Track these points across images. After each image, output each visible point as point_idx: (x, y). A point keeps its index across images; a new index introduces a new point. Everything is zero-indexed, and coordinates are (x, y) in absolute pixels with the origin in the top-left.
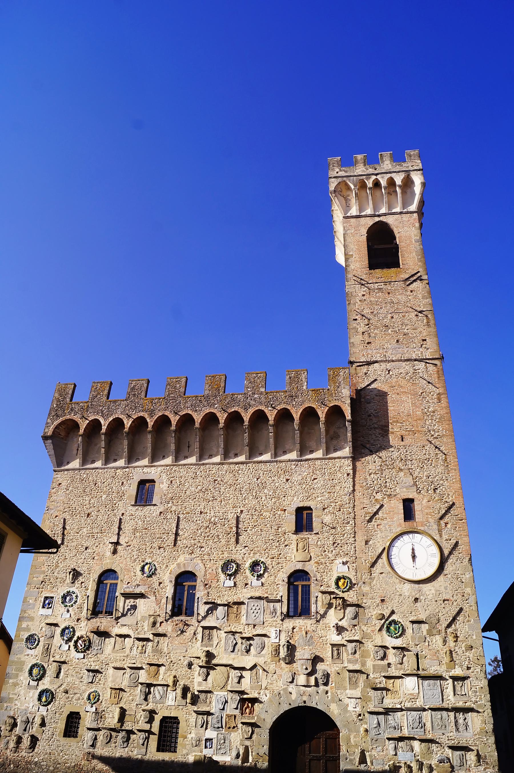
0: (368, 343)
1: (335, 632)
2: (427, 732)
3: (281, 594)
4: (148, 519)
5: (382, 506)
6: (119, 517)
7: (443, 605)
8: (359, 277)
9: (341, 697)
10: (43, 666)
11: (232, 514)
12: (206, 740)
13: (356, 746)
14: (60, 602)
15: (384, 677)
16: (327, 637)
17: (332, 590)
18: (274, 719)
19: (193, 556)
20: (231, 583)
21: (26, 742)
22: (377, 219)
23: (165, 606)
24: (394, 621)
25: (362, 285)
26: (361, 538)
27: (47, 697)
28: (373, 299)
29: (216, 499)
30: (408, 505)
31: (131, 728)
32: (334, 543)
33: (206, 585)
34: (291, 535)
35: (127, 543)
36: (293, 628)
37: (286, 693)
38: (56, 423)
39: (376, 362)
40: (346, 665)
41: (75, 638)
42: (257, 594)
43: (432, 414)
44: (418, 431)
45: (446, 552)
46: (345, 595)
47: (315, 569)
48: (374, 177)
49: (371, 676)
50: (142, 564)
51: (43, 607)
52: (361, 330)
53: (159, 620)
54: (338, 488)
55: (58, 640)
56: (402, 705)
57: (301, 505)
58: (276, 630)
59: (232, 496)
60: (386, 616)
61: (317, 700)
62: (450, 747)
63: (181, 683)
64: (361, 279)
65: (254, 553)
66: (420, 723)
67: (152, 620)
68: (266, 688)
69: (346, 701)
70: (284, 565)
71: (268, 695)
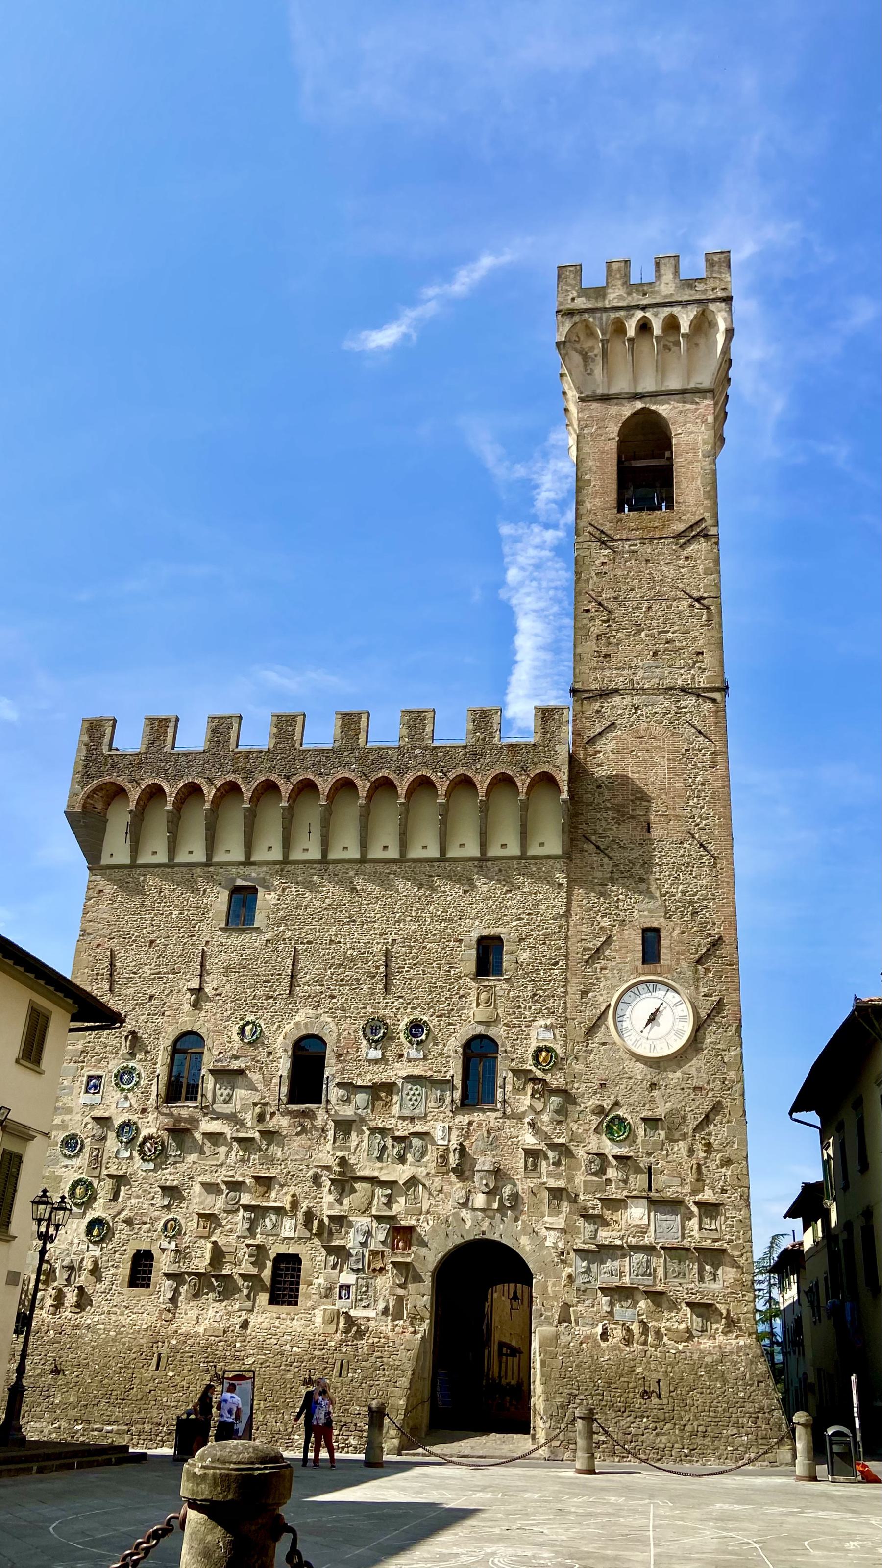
0: (606, 656)
1: (530, 1130)
2: (658, 1281)
3: (451, 1072)
4: (248, 951)
5: (609, 940)
6: (200, 948)
7: (692, 1096)
8: (599, 527)
9: (538, 1227)
10: (91, 1184)
11: (380, 946)
12: (341, 1287)
13: (556, 1297)
14: (113, 1083)
15: (599, 1199)
16: (520, 1138)
17: (529, 1068)
18: (440, 1256)
19: (320, 1011)
20: (375, 1054)
21: (71, 1298)
22: (639, 405)
23: (277, 1088)
24: (617, 1117)
25: (603, 543)
26: (574, 989)
27: (99, 1230)
28: (619, 573)
29: (354, 921)
30: (651, 939)
31: (229, 1273)
32: (535, 995)
33: (341, 1055)
34: (469, 980)
35: (216, 990)
36: (470, 1123)
37: (457, 1220)
38: (88, 788)
39: (616, 691)
40: (545, 1180)
41: (140, 1139)
42: (417, 1072)
43: (700, 787)
44: (677, 817)
45: (703, 1014)
46: (548, 1077)
47: (504, 1035)
48: (639, 314)
49: (582, 1197)
50: (241, 1023)
51: (87, 1092)
52: (595, 631)
53: (269, 1110)
54: (543, 907)
55: (112, 1143)
57: (486, 932)
58: (442, 1127)
59: (378, 916)
60: (607, 1108)
61: (503, 1232)
62: (688, 1304)
63: (304, 1206)
64: (602, 532)
65: (412, 1008)
66: (648, 1267)
67: (258, 1110)
68: (428, 1212)
69: (544, 1232)
70: (457, 1027)
71: (431, 1222)
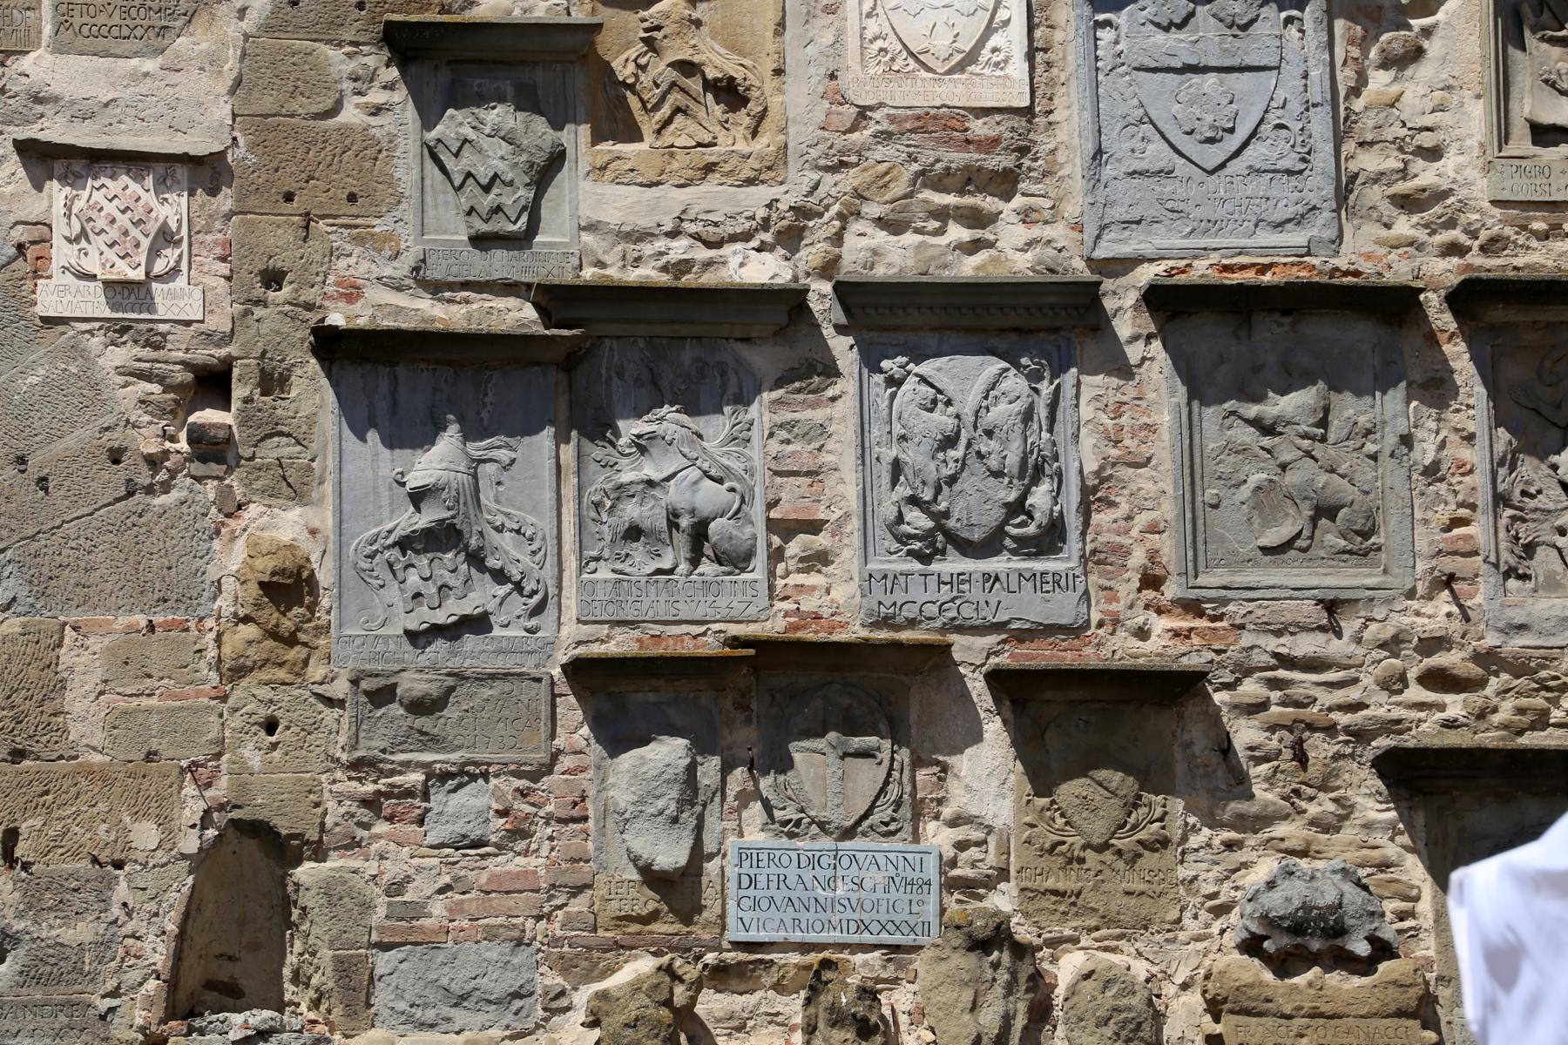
13: (143, 776)
56: (812, 253)
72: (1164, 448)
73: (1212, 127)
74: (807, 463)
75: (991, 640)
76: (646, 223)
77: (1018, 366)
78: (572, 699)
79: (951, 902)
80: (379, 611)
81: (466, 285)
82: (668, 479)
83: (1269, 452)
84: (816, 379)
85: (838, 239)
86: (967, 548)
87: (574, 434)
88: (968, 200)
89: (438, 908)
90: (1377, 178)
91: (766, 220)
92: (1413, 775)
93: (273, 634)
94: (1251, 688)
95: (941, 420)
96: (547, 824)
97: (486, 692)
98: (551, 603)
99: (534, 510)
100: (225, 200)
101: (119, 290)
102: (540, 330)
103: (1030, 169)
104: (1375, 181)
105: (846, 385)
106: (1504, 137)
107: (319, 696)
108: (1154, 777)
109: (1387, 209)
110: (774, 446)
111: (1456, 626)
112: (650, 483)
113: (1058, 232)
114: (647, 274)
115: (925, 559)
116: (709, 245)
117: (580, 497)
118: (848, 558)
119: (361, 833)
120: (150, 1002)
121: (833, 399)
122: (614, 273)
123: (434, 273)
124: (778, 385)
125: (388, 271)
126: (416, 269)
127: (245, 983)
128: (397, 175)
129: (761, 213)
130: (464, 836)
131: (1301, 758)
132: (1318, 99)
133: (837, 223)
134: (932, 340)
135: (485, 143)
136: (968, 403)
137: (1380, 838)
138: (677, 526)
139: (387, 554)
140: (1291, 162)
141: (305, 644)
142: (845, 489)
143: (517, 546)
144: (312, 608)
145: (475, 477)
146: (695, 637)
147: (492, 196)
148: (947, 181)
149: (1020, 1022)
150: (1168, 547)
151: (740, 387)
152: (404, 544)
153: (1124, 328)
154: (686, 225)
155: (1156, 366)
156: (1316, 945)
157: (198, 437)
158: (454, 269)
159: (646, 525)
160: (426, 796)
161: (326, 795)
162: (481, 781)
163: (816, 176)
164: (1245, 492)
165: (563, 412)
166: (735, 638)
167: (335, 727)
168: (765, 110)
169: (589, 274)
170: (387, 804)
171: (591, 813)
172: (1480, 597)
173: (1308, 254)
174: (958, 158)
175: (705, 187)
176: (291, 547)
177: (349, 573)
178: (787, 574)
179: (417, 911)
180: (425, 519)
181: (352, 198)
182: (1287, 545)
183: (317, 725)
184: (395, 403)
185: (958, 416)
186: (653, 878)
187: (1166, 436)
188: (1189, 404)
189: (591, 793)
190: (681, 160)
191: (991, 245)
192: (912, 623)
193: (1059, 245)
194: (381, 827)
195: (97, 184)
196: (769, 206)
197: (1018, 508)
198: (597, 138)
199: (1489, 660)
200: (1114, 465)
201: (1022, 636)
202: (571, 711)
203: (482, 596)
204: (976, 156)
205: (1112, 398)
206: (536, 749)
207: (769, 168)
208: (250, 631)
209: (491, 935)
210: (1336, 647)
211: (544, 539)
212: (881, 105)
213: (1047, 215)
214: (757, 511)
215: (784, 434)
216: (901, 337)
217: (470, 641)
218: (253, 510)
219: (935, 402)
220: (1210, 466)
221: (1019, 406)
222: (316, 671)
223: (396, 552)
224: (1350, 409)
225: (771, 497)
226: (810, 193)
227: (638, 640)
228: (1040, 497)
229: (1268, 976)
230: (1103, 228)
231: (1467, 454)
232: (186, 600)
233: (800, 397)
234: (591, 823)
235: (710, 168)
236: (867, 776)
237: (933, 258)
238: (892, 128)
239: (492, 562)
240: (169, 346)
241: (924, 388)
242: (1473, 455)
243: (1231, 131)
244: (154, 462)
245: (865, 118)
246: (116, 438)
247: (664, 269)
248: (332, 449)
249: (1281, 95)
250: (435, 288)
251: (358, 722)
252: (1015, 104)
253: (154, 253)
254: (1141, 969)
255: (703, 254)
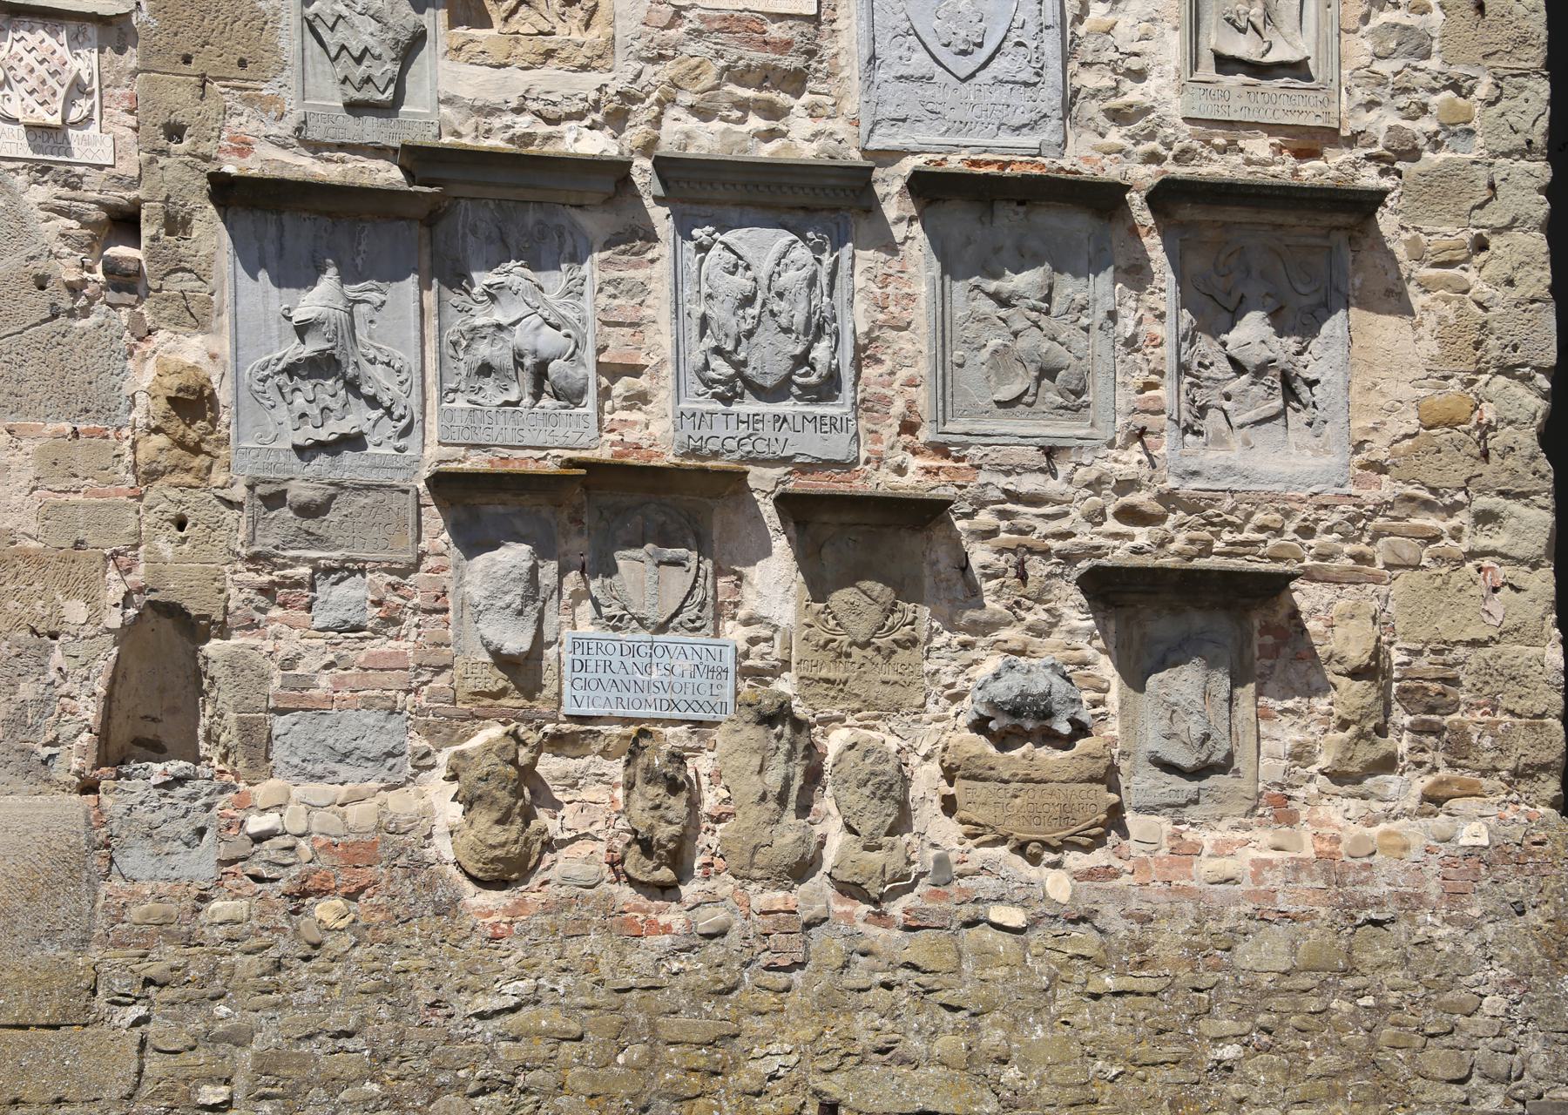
56: (635, 134)
72: (921, 315)
73: (966, 41)
74: (631, 316)
75: (779, 471)
76: (495, 99)
77: (804, 239)
78: (435, 509)
79: (744, 686)
80: (271, 428)
81: (341, 147)
82: (514, 324)
83: (1004, 321)
84: (638, 243)
85: (657, 122)
86: (761, 393)
87: (435, 281)
88: (765, 95)
89: (324, 681)
90: (1095, 94)
91: (597, 102)
92: (1108, 589)
93: (180, 443)
94: (985, 518)
95: (741, 282)
96: (414, 614)
97: (362, 501)
98: (417, 427)
99: (402, 346)
100: (131, 59)
101: (39, 133)
102: (406, 187)
103: (816, 70)
104: (1094, 96)
105: (663, 250)
106: (1195, 65)
107: (221, 499)
108: (908, 589)
109: (1102, 121)
110: (603, 300)
111: (1145, 471)
112: (499, 327)
113: (839, 126)
114: (496, 142)
115: (727, 401)
116: (549, 121)
117: (440, 337)
118: (663, 399)
119: (258, 616)
120: (84, 751)
121: (652, 261)
122: (467, 141)
123: (314, 134)
124: (607, 246)
125: (274, 130)
126: (299, 130)
127: (167, 741)
128: (281, 45)
129: (593, 95)
130: (345, 622)
131: (1023, 576)
132: (1050, 22)
133: (656, 108)
134: (734, 214)
135: (357, 19)
136: (764, 268)
137: (1081, 642)
138: (522, 365)
139: (277, 379)
140: (1028, 75)
141: (208, 454)
142: (661, 338)
143: (388, 377)
144: (214, 422)
145: (351, 314)
146: (537, 461)
147: (363, 67)
148: (748, 77)
149: (797, 783)
150: (923, 398)
151: (575, 247)
152: (291, 370)
153: (891, 210)
154: (529, 103)
155: (916, 246)
156: (1029, 725)
157: (111, 268)
158: (332, 131)
159: (495, 363)
160: (313, 588)
161: (229, 583)
162: (359, 576)
163: (639, 66)
164: (985, 354)
165: (426, 259)
166: (570, 460)
167: (235, 526)
168: (596, 5)
169: (447, 140)
170: (281, 593)
171: (450, 605)
172: (1164, 447)
173: (1039, 155)
174: (757, 57)
175: (545, 71)
176: (193, 368)
177: (245, 394)
178: (614, 410)
179: (306, 683)
180: (310, 348)
181: (242, 63)
182: (1017, 400)
183: (219, 524)
184: (282, 248)
185: (755, 280)
186: (503, 661)
187: (923, 304)
188: (942, 278)
189: (451, 589)
190: (525, 45)
191: (784, 135)
192: (715, 455)
193: (839, 137)
194: (276, 612)
195: (17, 36)
196: (599, 90)
197: (803, 360)
198: (454, 23)
199: (1169, 499)
200: (881, 327)
201: (806, 469)
202: (433, 519)
203: (358, 418)
204: (772, 56)
205: (881, 270)
206: (405, 551)
207: (600, 57)
208: (160, 440)
209: (368, 704)
210: (1052, 486)
211: (410, 371)
212: (694, 6)
213: (830, 110)
214: (589, 355)
215: (610, 290)
216: (709, 210)
217: (348, 457)
218: (161, 336)
219: (736, 266)
220: (957, 330)
221: (806, 273)
222: (218, 477)
223: (284, 378)
224: (1069, 288)
225: (600, 343)
226: (634, 81)
227: (490, 462)
228: (821, 352)
229: (992, 750)
230: (875, 123)
231: (1158, 330)
232: (105, 411)
233: (625, 258)
234: (451, 613)
235: (549, 54)
236: (678, 581)
237: (736, 143)
238: (702, 27)
239: (365, 390)
240: (85, 187)
241: (727, 254)
242: (1164, 331)
243: (980, 45)
244: (74, 289)
245: (680, 17)
246: (41, 266)
247: (511, 140)
248: (228, 285)
249: (1020, 17)
250: (316, 148)
251: (254, 522)
252: (806, 12)
253: (69, 102)
254: (893, 743)
255: (543, 129)
